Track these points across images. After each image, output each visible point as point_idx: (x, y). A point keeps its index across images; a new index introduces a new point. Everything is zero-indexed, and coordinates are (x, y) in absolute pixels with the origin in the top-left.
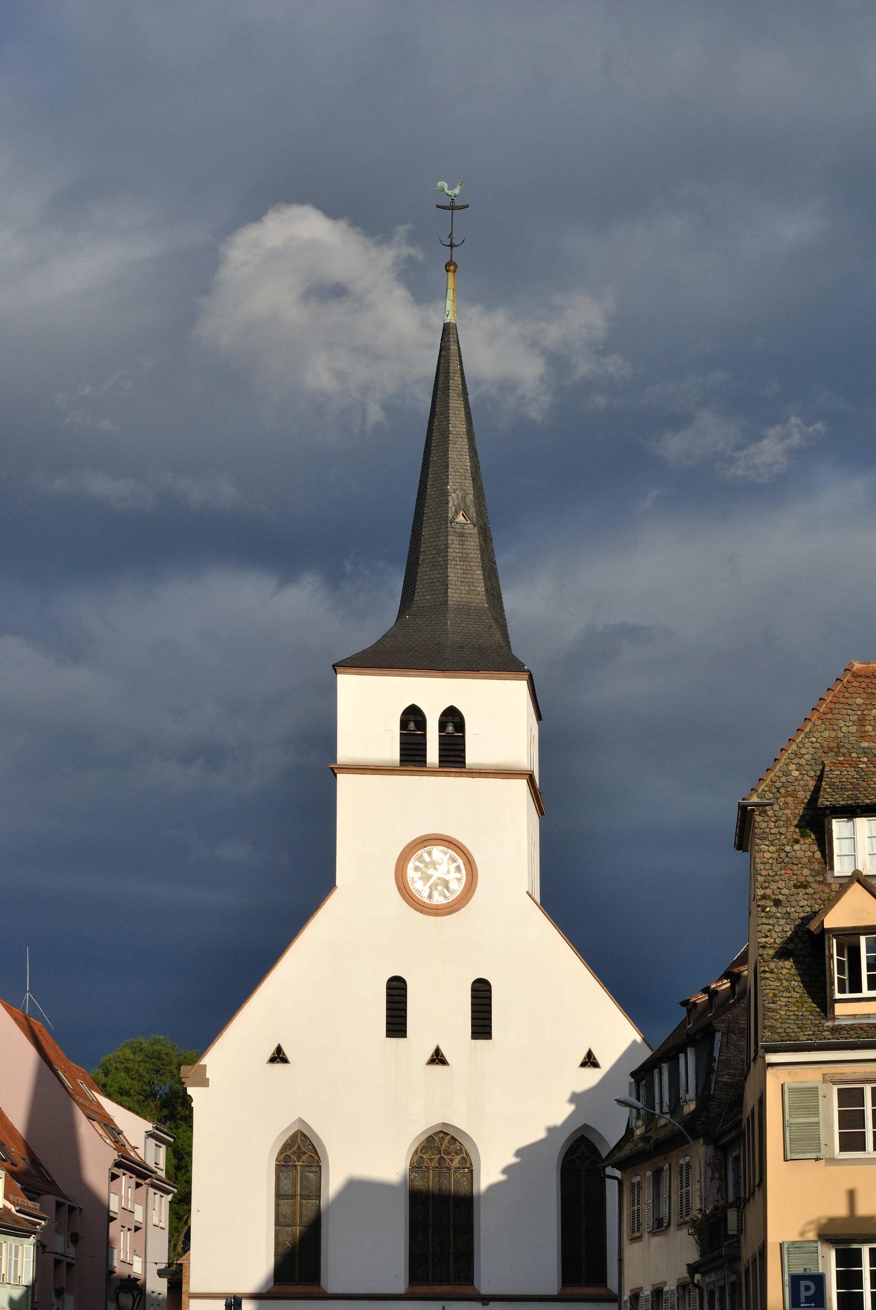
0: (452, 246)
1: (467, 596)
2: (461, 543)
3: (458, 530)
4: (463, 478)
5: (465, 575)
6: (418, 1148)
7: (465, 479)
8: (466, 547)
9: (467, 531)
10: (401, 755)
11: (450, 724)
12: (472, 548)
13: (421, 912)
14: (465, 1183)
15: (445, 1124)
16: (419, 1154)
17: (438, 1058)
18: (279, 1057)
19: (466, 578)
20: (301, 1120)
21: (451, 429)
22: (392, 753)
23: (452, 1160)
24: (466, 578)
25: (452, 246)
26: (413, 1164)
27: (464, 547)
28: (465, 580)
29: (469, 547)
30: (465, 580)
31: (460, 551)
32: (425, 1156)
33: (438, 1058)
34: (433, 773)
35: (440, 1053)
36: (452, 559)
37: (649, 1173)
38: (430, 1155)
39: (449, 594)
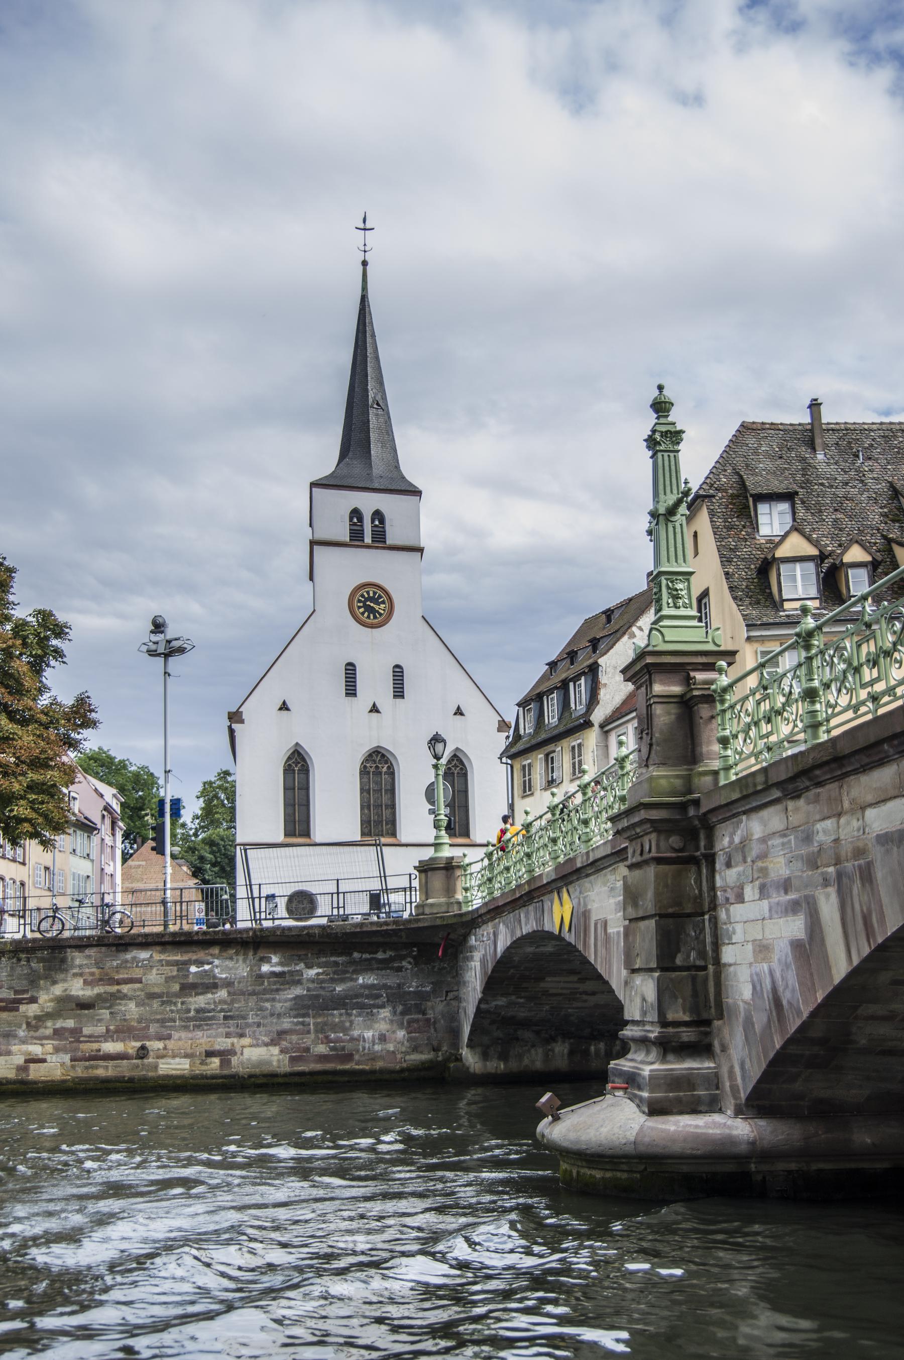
0: (365, 251)
17: (374, 709)
18: (284, 707)
20: (297, 744)
25: (365, 251)
33: (374, 709)
34: (368, 547)
37: (541, 756)
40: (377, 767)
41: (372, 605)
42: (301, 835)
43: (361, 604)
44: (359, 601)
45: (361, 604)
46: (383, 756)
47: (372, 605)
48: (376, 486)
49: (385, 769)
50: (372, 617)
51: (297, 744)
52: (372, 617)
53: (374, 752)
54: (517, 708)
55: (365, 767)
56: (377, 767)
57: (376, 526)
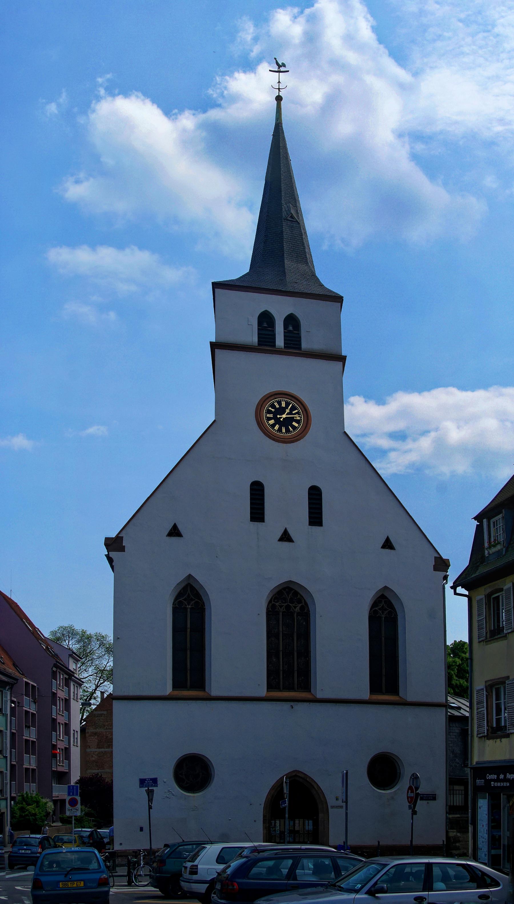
1: (296, 259)
2: (291, 230)
3: (288, 224)
4: (291, 198)
5: (294, 248)
6: (272, 598)
7: (292, 199)
8: (294, 233)
9: (294, 225)
10: (259, 341)
11: (290, 325)
12: (298, 234)
13: (273, 439)
14: (304, 623)
15: (290, 582)
16: (273, 603)
17: (286, 537)
19: (295, 249)
21: (282, 173)
22: (253, 339)
23: (295, 607)
24: (295, 249)
26: (269, 609)
27: (293, 233)
28: (295, 250)
29: (297, 233)
30: (295, 250)
31: (291, 234)
32: (277, 604)
33: (286, 537)
34: (279, 352)
35: (287, 534)
36: (286, 238)
38: (280, 604)
39: (285, 256)
40: (288, 607)
41: (284, 416)
42: (193, 687)
43: (271, 416)
44: (269, 412)
45: (271, 416)
46: (296, 593)
47: (284, 416)
48: (290, 289)
49: (298, 609)
50: (284, 430)
51: (190, 576)
52: (284, 430)
53: (284, 589)
54: (476, 523)
55: (274, 606)
56: (288, 607)
57: (290, 331)
